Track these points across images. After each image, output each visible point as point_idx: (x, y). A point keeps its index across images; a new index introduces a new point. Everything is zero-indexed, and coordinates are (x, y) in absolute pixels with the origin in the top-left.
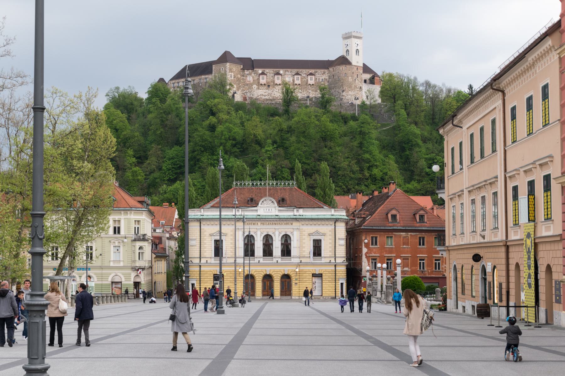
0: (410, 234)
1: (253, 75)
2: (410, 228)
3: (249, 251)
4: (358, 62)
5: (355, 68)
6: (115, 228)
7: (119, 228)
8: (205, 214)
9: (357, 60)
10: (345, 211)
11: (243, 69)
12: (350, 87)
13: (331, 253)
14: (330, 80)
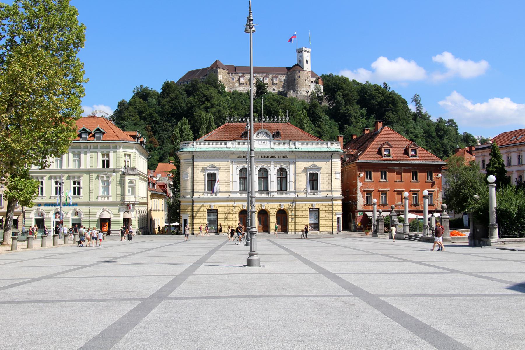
0: (403, 168)
2: (404, 162)
5: (306, 72)
6: (104, 161)
7: (108, 161)
11: (228, 73)
13: (327, 187)
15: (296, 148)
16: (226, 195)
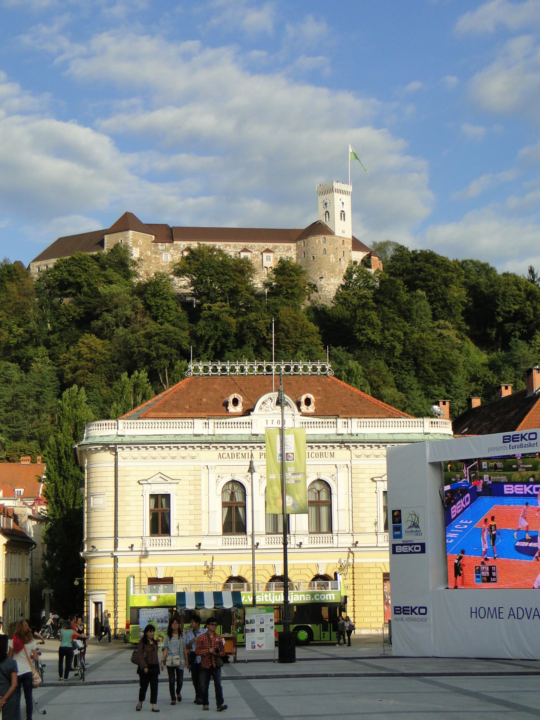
1: (172, 251)
3: (235, 522)
4: (343, 232)
8: (128, 432)
9: (343, 228)
10: (450, 425)
12: (333, 271)
14: (299, 260)
15: (352, 435)
16: (192, 544)
